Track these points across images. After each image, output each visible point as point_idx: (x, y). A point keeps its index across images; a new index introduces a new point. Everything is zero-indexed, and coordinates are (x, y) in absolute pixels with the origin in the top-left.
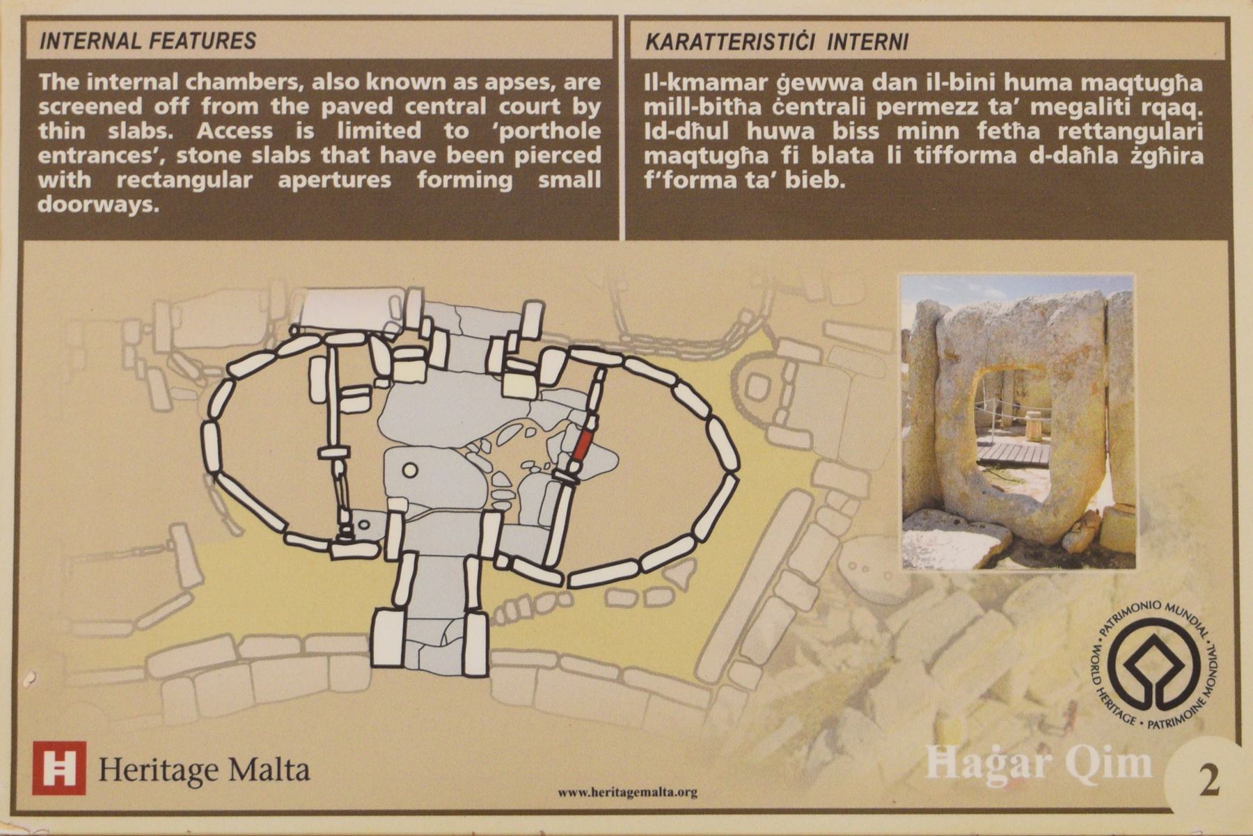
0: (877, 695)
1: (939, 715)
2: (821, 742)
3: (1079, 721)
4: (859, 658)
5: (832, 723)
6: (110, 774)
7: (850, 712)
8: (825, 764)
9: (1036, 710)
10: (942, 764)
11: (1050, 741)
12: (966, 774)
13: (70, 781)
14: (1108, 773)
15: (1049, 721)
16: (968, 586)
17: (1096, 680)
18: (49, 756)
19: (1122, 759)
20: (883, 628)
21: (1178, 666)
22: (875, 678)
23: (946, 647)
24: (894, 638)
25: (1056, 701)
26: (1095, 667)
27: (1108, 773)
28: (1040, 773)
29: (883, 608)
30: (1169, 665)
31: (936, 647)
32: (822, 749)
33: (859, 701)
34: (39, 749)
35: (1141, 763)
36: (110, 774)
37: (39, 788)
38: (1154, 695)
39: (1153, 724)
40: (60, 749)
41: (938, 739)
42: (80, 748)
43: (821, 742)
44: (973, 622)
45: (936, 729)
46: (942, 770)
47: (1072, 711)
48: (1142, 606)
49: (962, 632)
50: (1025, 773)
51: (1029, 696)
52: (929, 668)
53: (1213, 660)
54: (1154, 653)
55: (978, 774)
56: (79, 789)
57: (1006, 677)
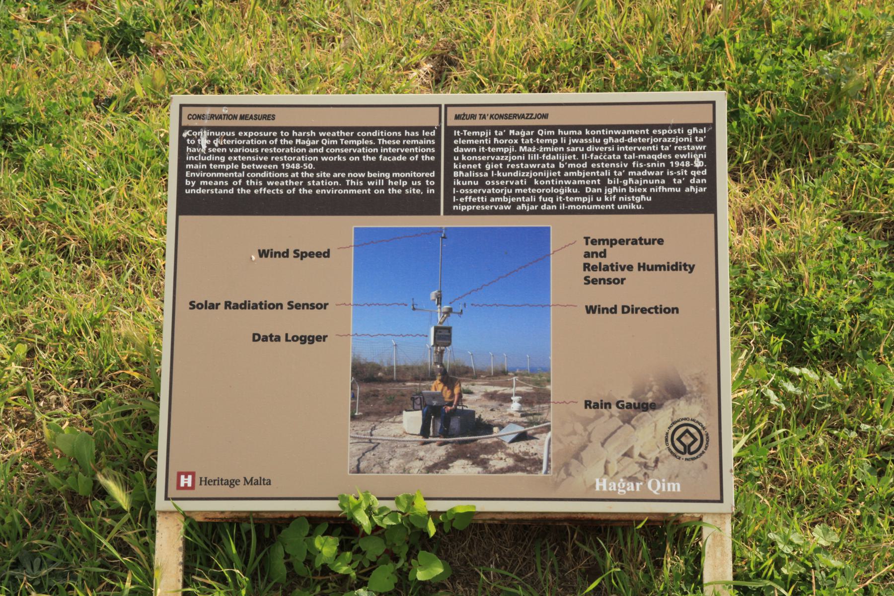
0: (583, 454)
1: (607, 462)
2: (562, 472)
3: (659, 464)
4: (576, 441)
5: (566, 465)
7: (574, 462)
8: (563, 480)
9: (643, 460)
10: (602, 485)
11: (649, 472)
12: (610, 489)
14: (664, 490)
15: (649, 464)
19: (669, 485)
20: (585, 430)
21: (695, 440)
22: (584, 447)
24: (590, 434)
25: (651, 457)
27: (664, 490)
28: (638, 489)
30: (692, 439)
31: (605, 437)
32: (563, 474)
33: (577, 456)
38: (687, 449)
39: (686, 459)
43: (562, 472)
44: (620, 427)
45: (606, 467)
46: (601, 487)
47: (657, 461)
48: (682, 419)
50: (633, 489)
51: (641, 455)
52: (603, 444)
53: (708, 438)
54: (683, 439)
55: (615, 489)
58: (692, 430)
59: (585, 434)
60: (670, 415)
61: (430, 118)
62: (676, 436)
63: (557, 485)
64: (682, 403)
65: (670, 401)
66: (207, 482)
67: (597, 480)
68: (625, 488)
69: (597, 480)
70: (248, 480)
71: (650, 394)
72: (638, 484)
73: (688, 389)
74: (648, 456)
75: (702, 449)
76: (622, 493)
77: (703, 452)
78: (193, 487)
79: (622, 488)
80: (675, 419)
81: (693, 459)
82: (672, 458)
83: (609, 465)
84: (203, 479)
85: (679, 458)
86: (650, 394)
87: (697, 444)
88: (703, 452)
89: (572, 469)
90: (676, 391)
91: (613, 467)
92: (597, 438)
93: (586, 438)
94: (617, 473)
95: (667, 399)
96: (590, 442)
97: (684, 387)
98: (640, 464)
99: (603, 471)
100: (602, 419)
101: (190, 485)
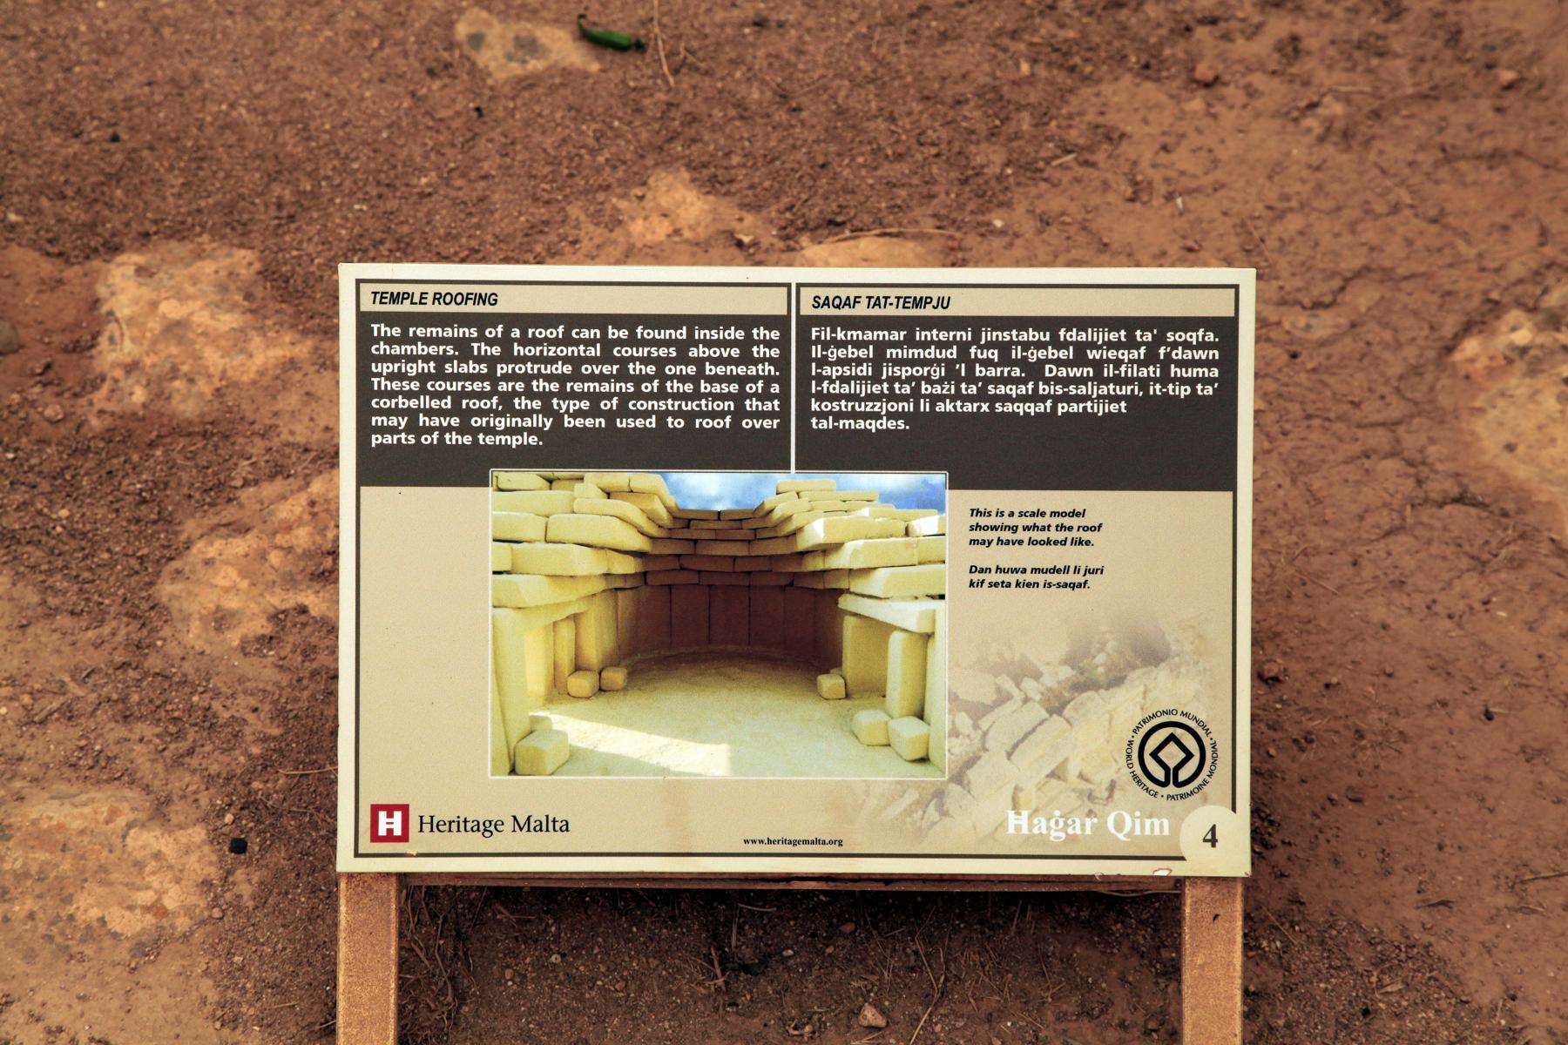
0: (972, 774)
1: (1016, 789)
2: (932, 807)
3: (1117, 794)
6: (427, 827)
7: (954, 789)
9: (1084, 785)
10: (1018, 824)
11: (1097, 808)
12: (1036, 831)
13: (398, 832)
14: (1138, 832)
15: (1097, 794)
16: (1038, 697)
17: (1130, 765)
18: (382, 815)
19: (1148, 822)
20: (976, 727)
21: (1189, 756)
22: (971, 762)
24: (985, 734)
25: (1102, 778)
26: (1129, 756)
29: (978, 712)
30: (1183, 755)
34: (375, 809)
35: (1161, 825)
36: (427, 827)
37: (375, 838)
38: (1171, 776)
40: (390, 810)
41: (1016, 807)
42: (404, 809)
43: (932, 807)
44: (1041, 723)
45: (1014, 798)
46: (1018, 828)
47: (1112, 787)
49: (1034, 730)
50: (1078, 832)
51: (1081, 776)
52: (1009, 755)
53: (1215, 752)
54: (1172, 747)
56: (404, 838)
57: (1066, 760)
59: (977, 736)
60: (1140, 699)
63: (920, 833)
64: (1161, 674)
65: (1138, 672)
71: (1101, 658)
73: (1174, 648)
74: (1096, 778)
83: (1021, 795)
85: (1155, 794)
86: (1101, 658)
89: (950, 803)
90: (1151, 655)
91: (1030, 794)
92: (998, 742)
93: (977, 742)
95: (1134, 667)
96: (986, 750)
97: (1167, 646)
98: (1081, 793)
100: (1008, 708)
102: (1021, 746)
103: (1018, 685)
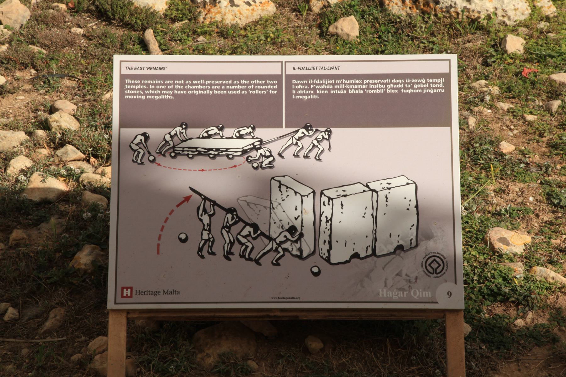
1: (386, 279)
3: (418, 280)
10: (384, 293)
15: (412, 280)
17: (422, 268)
19: (424, 293)
21: (440, 265)
22: (372, 270)
23: (387, 264)
25: (413, 276)
30: (437, 265)
33: (368, 276)
38: (435, 271)
46: (383, 295)
51: (406, 275)
52: (383, 269)
58: (438, 259)
61: (275, 70)
62: (428, 263)
66: (140, 293)
67: (380, 290)
68: (397, 295)
69: (380, 290)
70: (166, 291)
72: (405, 293)
73: (435, 234)
75: (444, 271)
76: (395, 298)
77: (445, 273)
78: (131, 296)
79: (396, 295)
80: (427, 253)
81: (438, 277)
82: (426, 276)
84: (138, 291)
87: (441, 268)
88: (445, 273)
91: (390, 283)
94: (392, 286)
98: (406, 280)
99: (384, 285)
101: (129, 295)
102: (387, 266)
103: (386, 247)
